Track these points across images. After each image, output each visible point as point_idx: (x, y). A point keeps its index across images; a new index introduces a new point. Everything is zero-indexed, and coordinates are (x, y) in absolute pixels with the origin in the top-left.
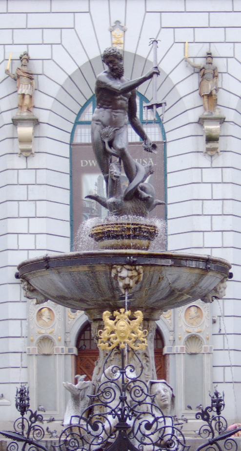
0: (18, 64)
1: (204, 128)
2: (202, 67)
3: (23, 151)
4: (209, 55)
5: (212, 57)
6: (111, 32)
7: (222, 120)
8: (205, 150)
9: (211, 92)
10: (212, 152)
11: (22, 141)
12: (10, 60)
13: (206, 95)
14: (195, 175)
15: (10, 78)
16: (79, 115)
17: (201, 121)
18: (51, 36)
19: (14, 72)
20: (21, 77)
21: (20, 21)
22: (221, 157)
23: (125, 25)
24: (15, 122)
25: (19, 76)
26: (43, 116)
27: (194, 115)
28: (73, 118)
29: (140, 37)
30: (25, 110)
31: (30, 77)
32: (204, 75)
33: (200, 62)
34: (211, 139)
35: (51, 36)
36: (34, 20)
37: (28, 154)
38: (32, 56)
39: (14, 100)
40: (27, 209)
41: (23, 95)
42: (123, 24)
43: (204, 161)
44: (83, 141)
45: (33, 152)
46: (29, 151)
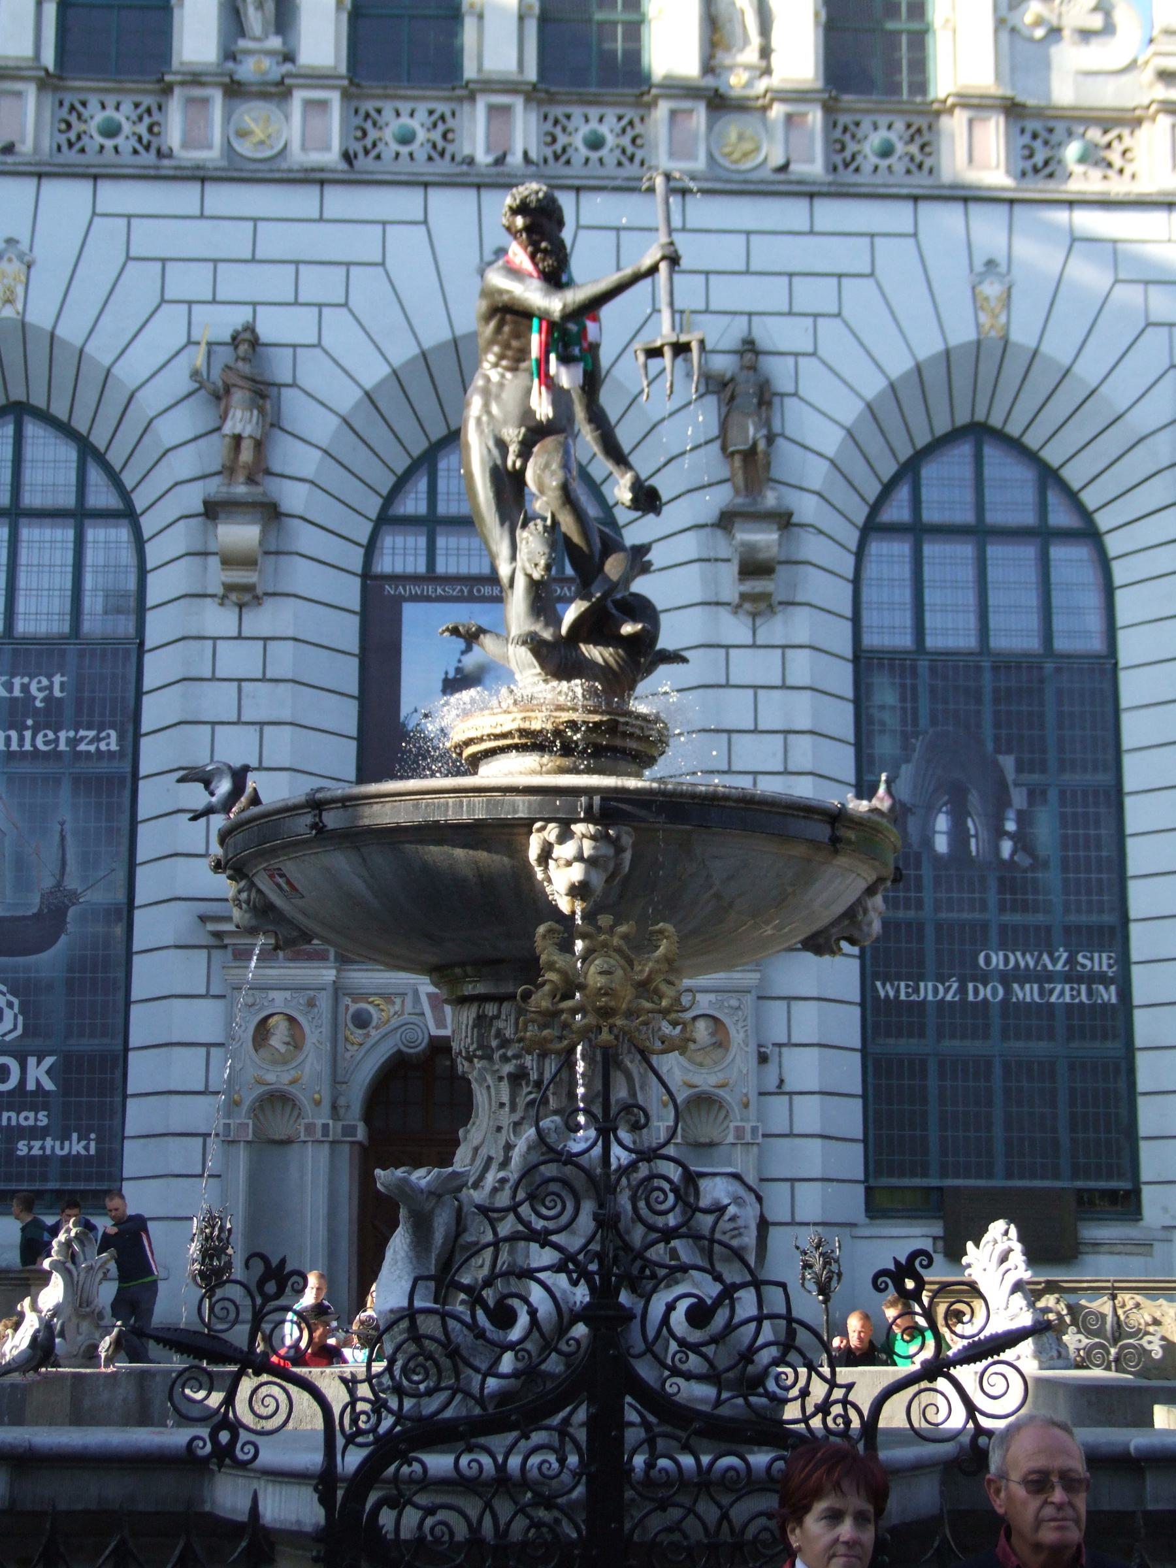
0: (224, 355)
1: (733, 538)
2: (728, 375)
3: (230, 588)
4: (749, 348)
7: (784, 520)
8: (735, 599)
9: (755, 444)
10: (758, 606)
11: (228, 561)
12: (203, 348)
13: (738, 452)
15: (203, 392)
16: (390, 499)
17: (726, 521)
18: (319, 284)
19: (216, 374)
20: (233, 390)
21: (236, 240)
22: (778, 619)
24: (212, 510)
25: (228, 389)
26: (293, 497)
28: (372, 507)
30: (242, 479)
31: (263, 393)
32: (732, 398)
33: (722, 364)
34: (754, 567)
36: (274, 241)
37: (247, 597)
38: (265, 332)
39: (214, 452)
41: (238, 439)
43: (736, 629)
44: (399, 569)
45: (259, 591)
46: (248, 588)
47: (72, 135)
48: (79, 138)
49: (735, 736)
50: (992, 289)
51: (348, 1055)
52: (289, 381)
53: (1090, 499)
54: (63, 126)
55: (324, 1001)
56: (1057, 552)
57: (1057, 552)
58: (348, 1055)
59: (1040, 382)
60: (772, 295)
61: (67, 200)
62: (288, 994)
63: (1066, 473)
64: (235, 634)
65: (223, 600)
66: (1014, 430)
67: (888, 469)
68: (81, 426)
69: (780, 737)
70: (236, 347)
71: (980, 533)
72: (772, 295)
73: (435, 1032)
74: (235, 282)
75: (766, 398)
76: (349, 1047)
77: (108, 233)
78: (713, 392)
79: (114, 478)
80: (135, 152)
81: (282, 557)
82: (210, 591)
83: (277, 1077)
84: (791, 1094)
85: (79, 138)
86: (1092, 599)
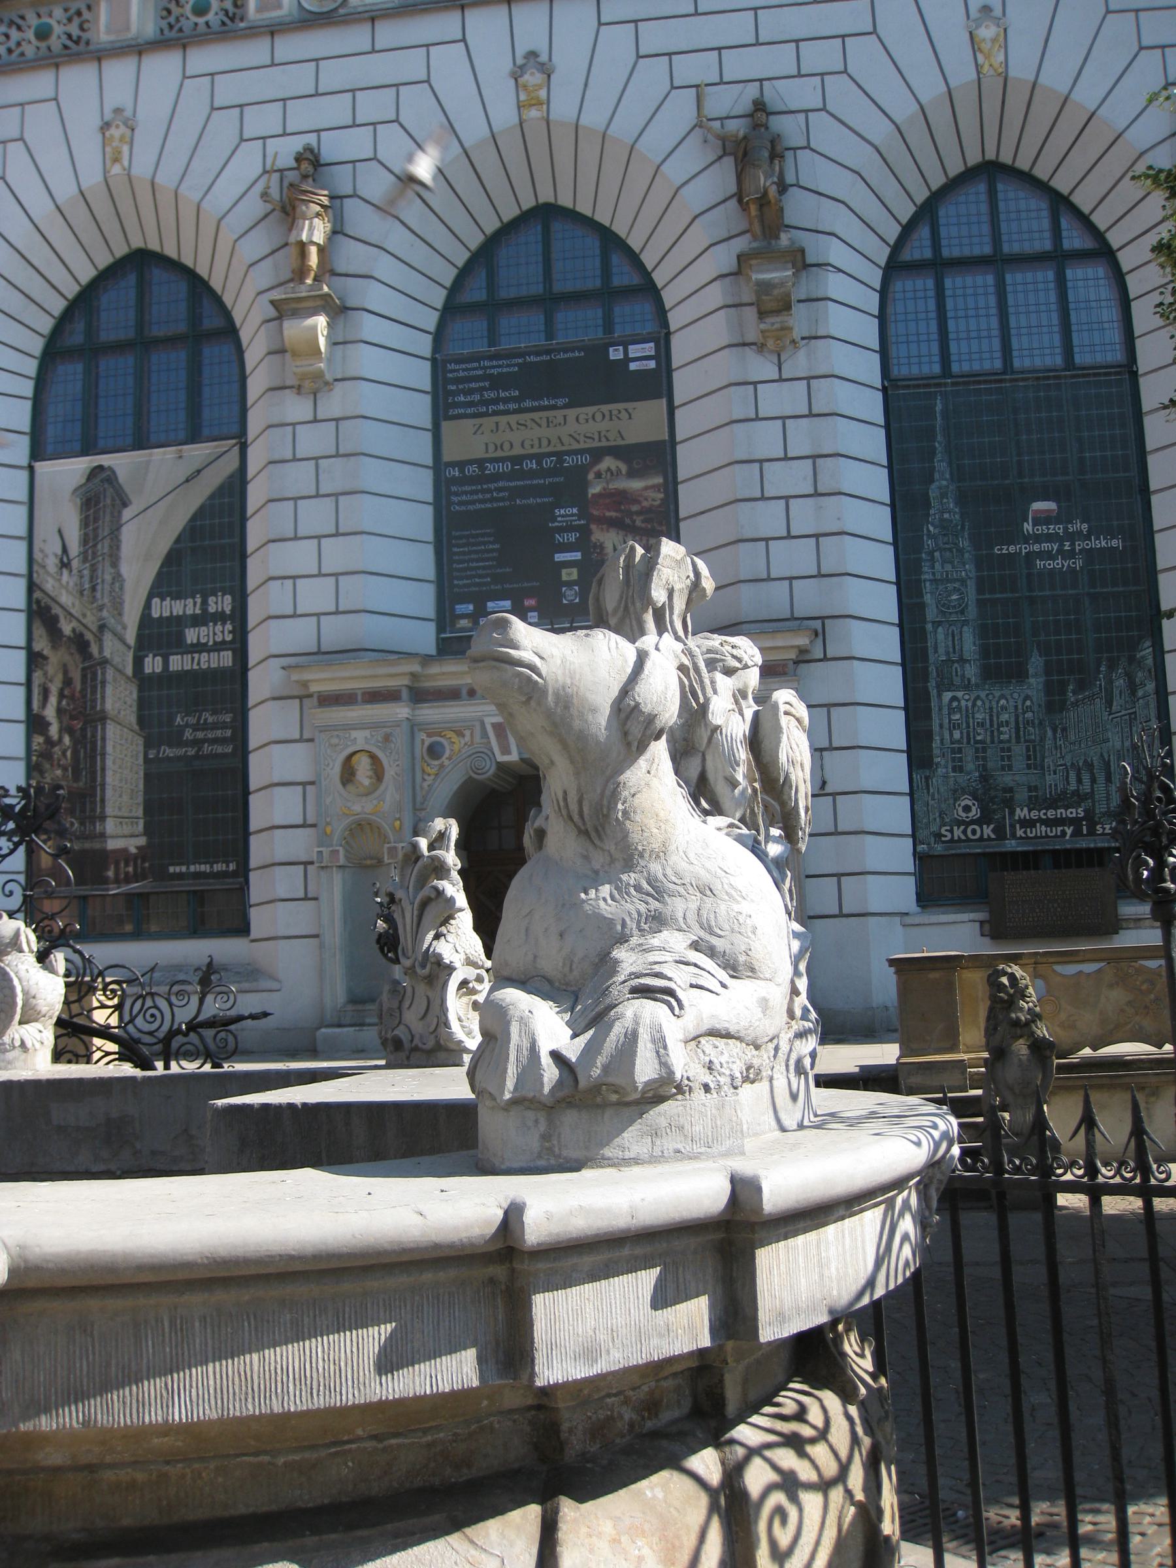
5: (769, 114)
6: (516, 80)
14: (738, 403)
21: (300, 79)
22: (801, 355)
23: (550, 60)
27: (724, 258)
29: (586, 85)
33: (736, 127)
35: (372, 106)
36: (334, 75)
38: (326, 155)
40: (315, 516)
42: (544, 58)
43: (764, 368)
45: (329, 377)
47: (172, 20)
48: (178, 20)
49: (766, 465)
50: (987, 32)
51: (425, 785)
52: (350, 192)
53: (1100, 220)
54: (165, 13)
55: (400, 739)
56: (1074, 273)
57: (1074, 273)
58: (425, 785)
59: (1043, 114)
60: (781, 60)
61: (163, 68)
62: (367, 733)
63: (1076, 199)
64: (311, 418)
65: (299, 389)
66: (1023, 164)
67: (906, 212)
68: (188, 261)
69: (810, 461)
70: (297, 169)
71: (998, 262)
72: (781, 60)
73: (501, 758)
74: (303, 116)
75: (777, 151)
76: (426, 777)
77: (197, 90)
78: (730, 154)
79: (217, 300)
80: (223, 24)
81: (349, 346)
82: (288, 383)
83: (361, 807)
84: (834, 795)
85: (178, 20)
86: (1110, 314)
